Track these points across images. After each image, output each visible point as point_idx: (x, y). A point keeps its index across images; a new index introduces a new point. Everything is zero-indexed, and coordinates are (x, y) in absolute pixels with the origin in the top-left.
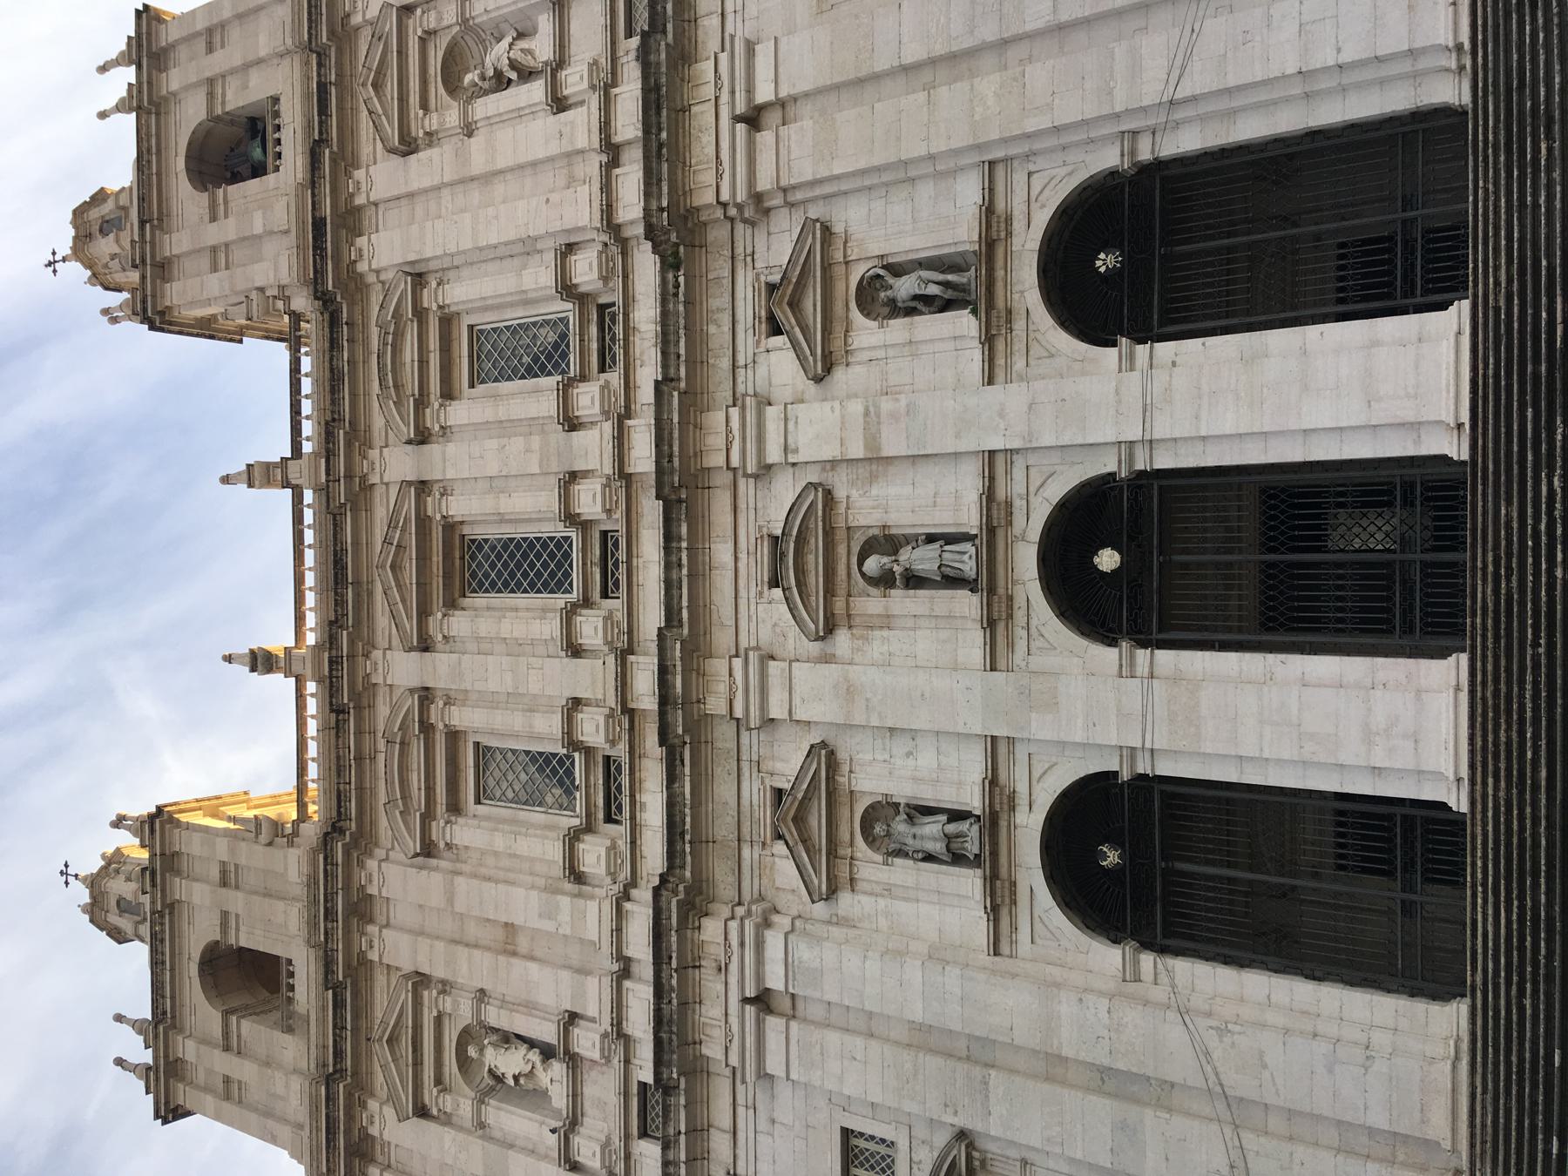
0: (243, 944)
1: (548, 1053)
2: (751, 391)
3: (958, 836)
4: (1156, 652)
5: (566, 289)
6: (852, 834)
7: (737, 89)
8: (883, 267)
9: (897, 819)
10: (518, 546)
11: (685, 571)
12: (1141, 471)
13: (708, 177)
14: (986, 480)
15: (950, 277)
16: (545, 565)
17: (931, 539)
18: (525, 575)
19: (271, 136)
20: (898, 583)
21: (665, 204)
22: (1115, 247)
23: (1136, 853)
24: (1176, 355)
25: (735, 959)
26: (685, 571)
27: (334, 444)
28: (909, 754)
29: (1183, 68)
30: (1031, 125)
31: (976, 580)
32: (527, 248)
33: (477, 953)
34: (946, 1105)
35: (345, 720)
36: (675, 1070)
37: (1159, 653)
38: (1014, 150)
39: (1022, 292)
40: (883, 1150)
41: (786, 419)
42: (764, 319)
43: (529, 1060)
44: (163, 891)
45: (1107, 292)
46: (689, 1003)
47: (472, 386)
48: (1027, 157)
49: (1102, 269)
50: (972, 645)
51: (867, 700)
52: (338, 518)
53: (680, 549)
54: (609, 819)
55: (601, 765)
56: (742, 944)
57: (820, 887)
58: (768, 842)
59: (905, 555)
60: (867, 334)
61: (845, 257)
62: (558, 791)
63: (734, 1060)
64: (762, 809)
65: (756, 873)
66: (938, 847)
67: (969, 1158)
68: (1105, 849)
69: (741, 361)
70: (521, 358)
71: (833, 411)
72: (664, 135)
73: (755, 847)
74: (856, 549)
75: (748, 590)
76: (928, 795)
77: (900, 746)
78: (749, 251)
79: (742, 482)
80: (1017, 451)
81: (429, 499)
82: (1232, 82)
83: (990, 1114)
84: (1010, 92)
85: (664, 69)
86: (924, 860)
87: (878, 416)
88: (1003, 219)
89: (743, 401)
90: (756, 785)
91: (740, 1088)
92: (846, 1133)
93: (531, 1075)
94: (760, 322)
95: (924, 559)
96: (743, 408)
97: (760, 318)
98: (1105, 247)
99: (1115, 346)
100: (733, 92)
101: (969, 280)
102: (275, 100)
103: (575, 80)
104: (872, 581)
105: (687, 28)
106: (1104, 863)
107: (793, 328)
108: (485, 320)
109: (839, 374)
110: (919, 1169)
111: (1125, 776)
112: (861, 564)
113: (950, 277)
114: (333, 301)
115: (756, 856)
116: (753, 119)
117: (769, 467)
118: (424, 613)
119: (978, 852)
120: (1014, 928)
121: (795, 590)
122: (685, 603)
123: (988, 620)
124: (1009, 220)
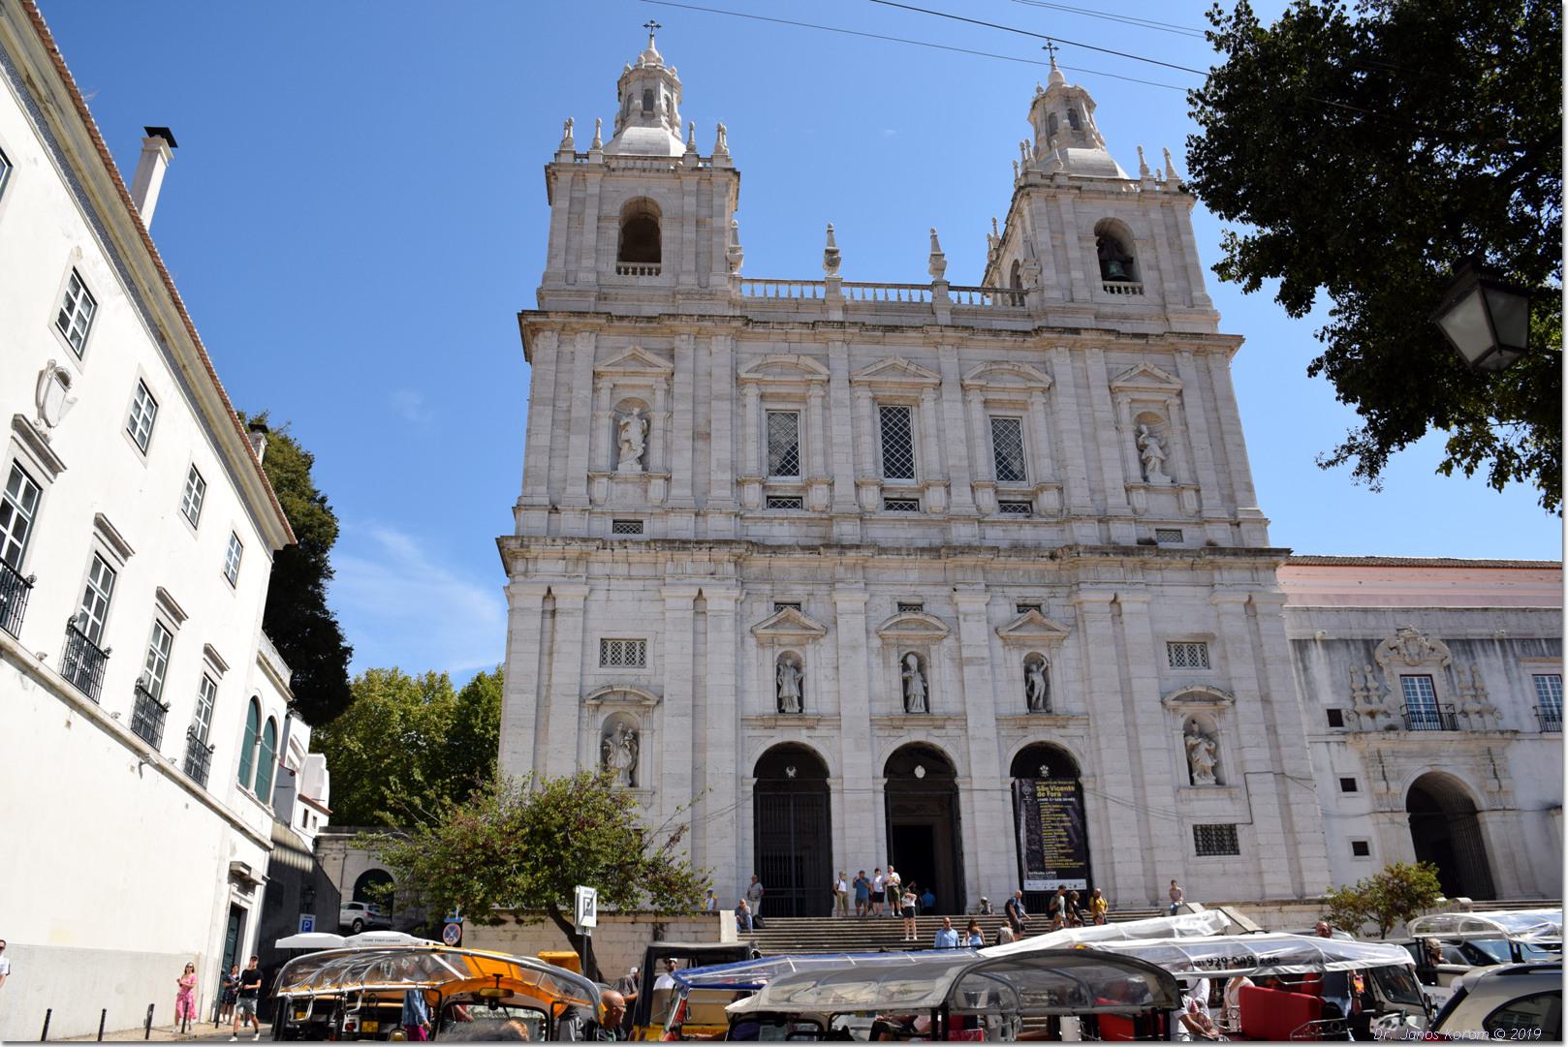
5: (1042, 488)
6: (784, 645)
8: (1047, 668)
15: (1041, 701)
16: (898, 460)
17: (926, 689)
18: (892, 446)
30: (1103, 741)
32: (1059, 462)
33: (690, 416)
38: (1092, 731)
40: (637, 659)
50: (881, 709)
59: (918, 677)
60: (1016, 661)
62: (778, 465)
66: (785, 692)
67: (649, 706)
76: (808, 686)
77: (830, 672)
80: (966, 732)
82: (1112, 822)
95: (916, 687)
103: (1140, 499)
104: (904, 661)
108: (1024, 426)
109: (999, 642)
113: (1041, 701)
114: (1037, 334)
117: (956, 604)
124: (1064, 727)
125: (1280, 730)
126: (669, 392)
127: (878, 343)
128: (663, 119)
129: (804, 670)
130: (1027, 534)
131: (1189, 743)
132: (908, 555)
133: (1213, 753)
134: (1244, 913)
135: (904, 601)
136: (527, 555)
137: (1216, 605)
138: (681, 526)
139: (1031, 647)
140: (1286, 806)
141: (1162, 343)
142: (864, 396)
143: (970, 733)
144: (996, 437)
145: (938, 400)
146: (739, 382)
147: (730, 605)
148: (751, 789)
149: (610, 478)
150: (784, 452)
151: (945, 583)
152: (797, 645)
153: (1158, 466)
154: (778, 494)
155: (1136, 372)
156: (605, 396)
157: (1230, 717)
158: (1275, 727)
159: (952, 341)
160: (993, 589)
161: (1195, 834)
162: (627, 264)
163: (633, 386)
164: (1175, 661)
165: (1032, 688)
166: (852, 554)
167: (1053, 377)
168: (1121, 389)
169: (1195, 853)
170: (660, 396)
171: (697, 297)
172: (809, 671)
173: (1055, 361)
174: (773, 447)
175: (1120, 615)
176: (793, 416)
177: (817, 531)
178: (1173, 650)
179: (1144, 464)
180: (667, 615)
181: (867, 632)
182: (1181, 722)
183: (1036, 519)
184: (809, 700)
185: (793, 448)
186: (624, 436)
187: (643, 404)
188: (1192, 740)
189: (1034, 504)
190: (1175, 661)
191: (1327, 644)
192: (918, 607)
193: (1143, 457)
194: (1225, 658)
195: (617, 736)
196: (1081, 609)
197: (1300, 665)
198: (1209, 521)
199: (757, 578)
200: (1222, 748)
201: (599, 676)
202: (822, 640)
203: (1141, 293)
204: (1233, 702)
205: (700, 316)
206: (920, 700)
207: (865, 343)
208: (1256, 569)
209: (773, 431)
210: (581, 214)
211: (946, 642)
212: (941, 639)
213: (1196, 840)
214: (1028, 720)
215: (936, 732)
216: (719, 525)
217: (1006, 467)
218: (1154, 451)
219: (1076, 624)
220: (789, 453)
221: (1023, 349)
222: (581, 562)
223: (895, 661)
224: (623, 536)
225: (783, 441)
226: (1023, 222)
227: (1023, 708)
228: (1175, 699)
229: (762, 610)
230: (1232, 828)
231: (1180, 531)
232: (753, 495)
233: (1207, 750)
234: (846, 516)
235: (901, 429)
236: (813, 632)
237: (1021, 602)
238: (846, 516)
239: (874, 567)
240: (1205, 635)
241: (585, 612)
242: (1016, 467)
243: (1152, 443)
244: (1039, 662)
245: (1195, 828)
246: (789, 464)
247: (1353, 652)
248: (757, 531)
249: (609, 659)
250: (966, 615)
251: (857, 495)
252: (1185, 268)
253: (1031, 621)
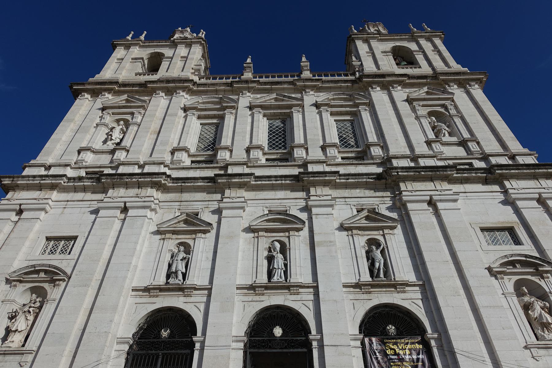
0: (163, 62)
1: (118, 144)
2: (337, 203)
3: (177, 277)
4: (242, 351)
7: (441, 196)
8: (383, 247)
9: (185, 254)
11: (274, 182)
12: (312, 344)
13: (410, 188)
14: (308, 285)
19: (409, 66)
20: (269, 253)
21: (400, 173)
22: (397, 333)
23: (167, 344)
24: (357, 357)
25: (140, 200)
26: (274, 182)
27: (315, 81)
28: (207, 258)
29: (468, 357)
31: (270, 282)
34: (79, 272)
35: (228, 86)
36: (105, 180)
39: (378, 297)
40: (68, 251)
41: (328, 214)
42: (362, 207)
43: (116, 139)
44: (181, 42)
45: (379, 330)
46: (127, 186)
47: (335, 121)
49: (388, 328)
51: (228, 243)
52: (292, 83)
53: (282, 180)
54: (192, 162)
55: (210, 159)
56: (144, 202)
57: (162, 228)
58: (180, 211)
59: (280, 256)
61: (386, 234)
62: (203, 147)
63: (106, 200)
64: (191, 209)
65: (170, 207)
68: (168, 331)
69: (347, 200)
70: (344, 134)
71: (331, 230)
72: (423, 173)
73: (178, 206)
74: (282, 239)
75: (268, 203)
76: (192, 265)
78: (386, 202)
81: (298, 108)
83: (74, 287)
84: (451, 291)
85: (445, 173)
86: (169, 264)
87: (330, 246)
88: (404, 290)
89: (334, 200)
90: (200, 207)
91: (96, 202)
92: (75, 238)
93: (111, 139)
94: (361, 206)
96: (331, 200)
97: (363, 206)
98: (397, 329)
99: (360, 333)
100: (440, 195)
101: (381, 278)
102: (420, 67)
103: (437, 147)
105: (459, 181)
106: (163, 331)
107: (360, 216)
110: (59, 262)
111: (195, 339)
112: (277, 241)
115: (175, 207)
116: (431, 203)
118: (262, 107)
119: (170, 283)
120: (141, 297)
121: (267, 218)
123: (255, 286)
124: (404, 292)
164: (490, 242)
220: (210, 141)
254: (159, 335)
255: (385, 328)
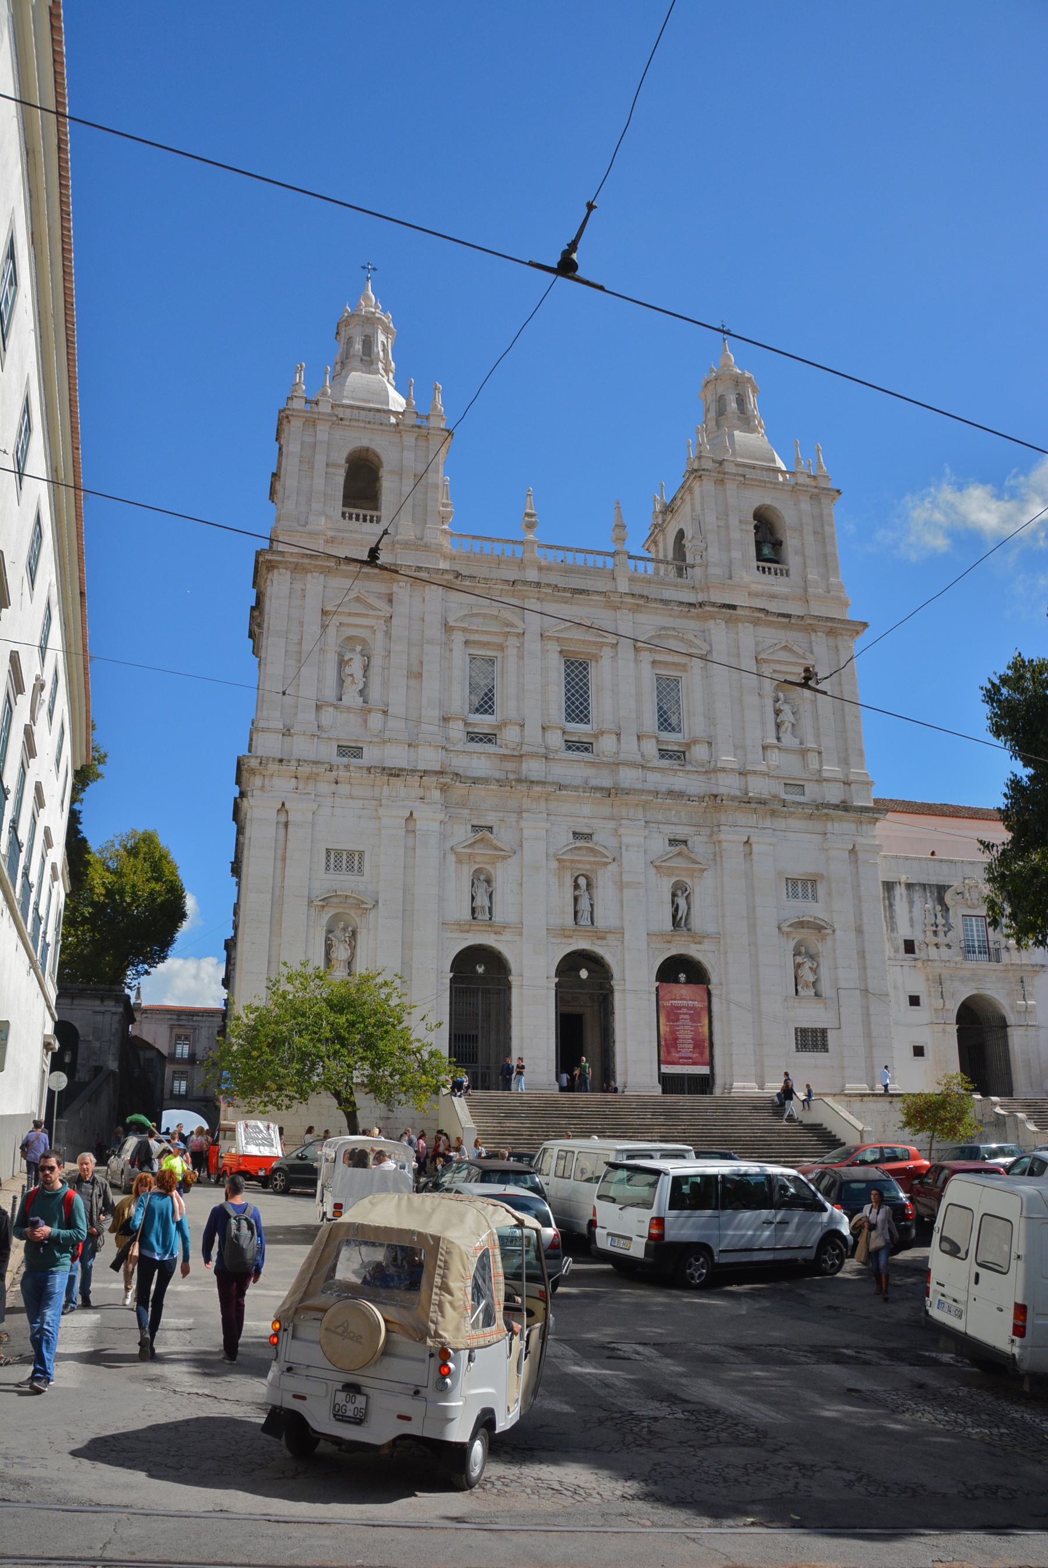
6: (479, 863)
10: (586, 692)
16: (577, 708)
17: (592, 905)
37: (554, 992)
40: (356, 868)
48: (719, 950)
59: (586, 895)
60: (666, 886)
66: (478, 902)
67: (366, 909)
69: (661, 826)
74: (588, 874)
79: (613, 822)
86: (472, 896)
95: (584, 904)
104: (576, 881)
108: (683, 685)
109: (653, 871)
112: (583, 875)
122: (569, 792)
124: (700, 943)
125: (867, 956)
126: (388, 634)
127: (566, 603)
128: (380, 365)
129: (494, 884)
130: (679, 782)
131: (796, 962)
132: (584, 792)
133: (814, 971)
134: (836, 1101)
135: (577, 830)
136: (264, 772)
137: (827, 850)
138: (397, 756)
139: (678, 876)
140: (867, 1014)
141: (802, 623)
142: (554, 647)
143: (626, 942)
144: (659, 693)
145: (614, 658)
146: (448, 629)
147: (435, 826)
148: (448, 981)
149: (336, 707)
150: (482, 694)
151: (612, 818)
152: (489, 863)
153: (790, 728)
154: (476, 730)
155: (777, 647)
156: (332, 631)
157: (829, 941)
158: (864, 952)
159: (629, 607)
160: (651, 825)
161: (796, 1034)
162: (352, 510)
163: (356, 626)
164: (790, 894)
165: (676, 910)
166: (537, 789)
167: (711, 645)
168: (765, 661)
169: (795, 1049)
170: (380, 635)
171: (413, 548)
172: (498, 884)
173: (713, 631)
174: (473, 688)
175: (751, 854)
176: (491, 661)
177: (509, 766)
178: (790, 885)
179: (778, 726)
180: (383, 831)
181: (547, 855)
182: (792, 944)
183: (688, 768)
184: (497, 909)
185: (490, 691)
186: (348, 670)
187: (363, 642)
188: (799, 959)
189: (687, 753)
190: (790, 894)
191: (909, 886)
192: (588, 837)
193: (778, 721)
194: (829, 894)
195: (338, 932)
196: (720, 847)
197: (887, 902)
198: (826, 780)
199: (457, 804)
200: (821, 967)
201: (326, 882)
202: (509, 860)
203: (787, 575)
204: (834, 931)
205: (418, 567)
206: (587, 914)
207: (556, 601)
208: (861, 822)
209: (473, 674)
210: (311, 463)
211: (610, 867)
212: (606, 864)
213: (796, 1039)
214: (673, 936)
215: (599, 942)
216: (429, 758)
217: (666, 721)
218: (787, 716)
219: (717, 857)
220: (486, 694)
221: (686, 617)
222: (310, 781)
223: (569, 882)
224: (345, 760)
225: (482, 683)
226: (692, 499)
227: (668, 926)
228: (789, 926)
229: (462, 833)
230: (824, 1031)
231: (803, 786)
232: (457, 731)
233: (811, 968)
234: (533, 755)
235: (581, 680)
236: (503, 853)
237: (672, 838)
238: (533, 755)
239: (555, 800)
240: (816, 875)
241: (313, 824)
242: (674, 721)
243: (786, 708)
244: (683, 889)
245: (796, 1029)
246: (486, 705)
247: (928, 894)
248: (459, 763)
249: (332, 866)
250: (628, 846)
251: (543, 736)
252: (825, 556)
253: (679, 854)
254: (475, 971)
255: (677, 976)
